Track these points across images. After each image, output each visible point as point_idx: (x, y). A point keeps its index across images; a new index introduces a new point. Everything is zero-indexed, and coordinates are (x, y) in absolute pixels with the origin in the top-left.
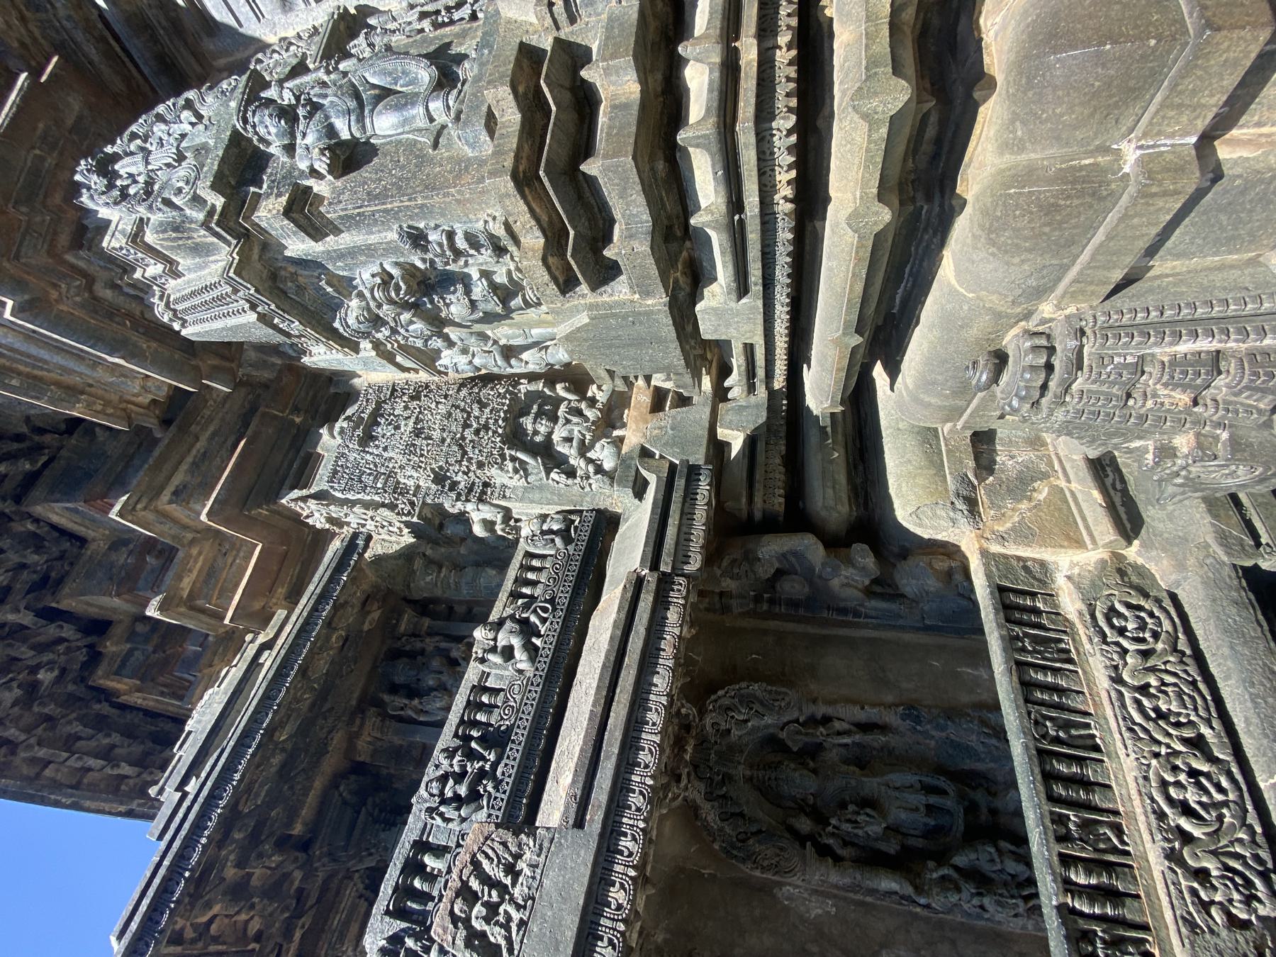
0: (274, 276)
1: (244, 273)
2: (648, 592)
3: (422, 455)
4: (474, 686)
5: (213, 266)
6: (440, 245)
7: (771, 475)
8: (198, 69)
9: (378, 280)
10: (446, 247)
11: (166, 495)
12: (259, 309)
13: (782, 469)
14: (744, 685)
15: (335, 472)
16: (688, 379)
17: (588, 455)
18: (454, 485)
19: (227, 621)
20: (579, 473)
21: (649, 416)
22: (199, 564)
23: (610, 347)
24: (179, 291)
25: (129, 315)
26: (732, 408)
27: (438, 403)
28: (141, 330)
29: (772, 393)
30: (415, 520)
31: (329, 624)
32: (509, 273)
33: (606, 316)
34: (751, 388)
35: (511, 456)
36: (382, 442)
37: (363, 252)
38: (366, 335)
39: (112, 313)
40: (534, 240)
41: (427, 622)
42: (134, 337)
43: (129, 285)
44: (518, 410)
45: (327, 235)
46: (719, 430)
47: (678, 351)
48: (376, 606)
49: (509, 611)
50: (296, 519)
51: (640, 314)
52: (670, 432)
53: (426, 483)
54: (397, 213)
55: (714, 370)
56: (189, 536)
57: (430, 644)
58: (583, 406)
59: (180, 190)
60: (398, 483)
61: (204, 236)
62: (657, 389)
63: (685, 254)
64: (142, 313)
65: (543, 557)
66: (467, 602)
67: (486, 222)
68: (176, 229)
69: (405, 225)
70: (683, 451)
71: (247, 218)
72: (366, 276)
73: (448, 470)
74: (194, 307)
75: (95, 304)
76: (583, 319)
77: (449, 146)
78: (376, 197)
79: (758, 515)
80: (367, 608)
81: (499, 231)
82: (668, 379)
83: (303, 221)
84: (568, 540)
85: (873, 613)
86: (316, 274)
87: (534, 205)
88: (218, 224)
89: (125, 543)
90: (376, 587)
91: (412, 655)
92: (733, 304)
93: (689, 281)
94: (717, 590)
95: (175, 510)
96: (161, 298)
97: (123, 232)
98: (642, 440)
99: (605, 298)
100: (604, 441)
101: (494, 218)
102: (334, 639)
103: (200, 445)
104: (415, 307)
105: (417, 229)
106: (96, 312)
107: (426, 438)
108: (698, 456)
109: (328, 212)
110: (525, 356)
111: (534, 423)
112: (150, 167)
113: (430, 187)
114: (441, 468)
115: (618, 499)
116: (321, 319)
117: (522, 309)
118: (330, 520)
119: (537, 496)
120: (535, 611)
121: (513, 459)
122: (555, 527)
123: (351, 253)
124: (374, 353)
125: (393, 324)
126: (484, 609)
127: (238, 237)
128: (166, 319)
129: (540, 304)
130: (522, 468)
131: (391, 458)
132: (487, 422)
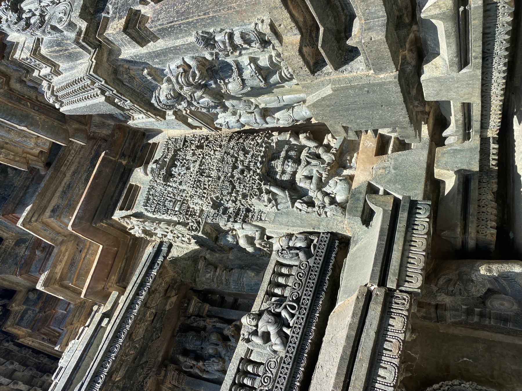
0: (115, 72)
1: (99, 71)
2: (376, 303)
3: (205, 188)
4: (242, 359)
5: (80, 67)
6: (224, 43)
7: (484, 210)
9: (181, 70)
10: (227, 45)
11: (48, 213)
12: (107, 94)
13: (494, 204)
14: (456, 382)
15: (148, 199)
16: (411, 131)
17: (324, 189)
18: (226, 209)
19: (82, 296)
20: (317, 203)
21: (375, 158)
22: (66, 257)
23: (347, 110)
24: (59, 84)
25: (29, 99)
26: (448, 152)
27: (215, 151)
28: (36, 108)
29: (484, 141)
30: (200, 234)
31: (145, 304)
32: (271, 57)
33: (347, 88)
34: (466, 136)
35: (266, 189)
36: (178, 179)
37: (172, 54)
38: (171, 107)
39: (20, 98)
40: (293, 38)
41: (207, 307)
42: (33, 113)
43: (30, 80)
44: (272, 155)
45: (149, 42)
46: (436, 170)
47: (404, 111)
48: (173, 293)
49: (265, 306)
50: (124, 231)
51: (374, 85)
52: (393, 171)
53: (207, 209)
54: (195, 24)
55: (431, 120)
56: (60, 239)
57: (209, 323)
58: (320, 151)
59: (61, 20)
60: (189, 207)
61: (75, 48)
62: (382, 136)
63: (412, 35)
64: (36, 97)
65: (290, 266)
66: (235, 294)
67: (256, 24)
68: (58, 45)
69: (200, 31)
70: (404, 188)
71: (101, 35)
72: (173, 67)
73: (222, 199)
74: (68, 94)
75: (11, 94)
76: (328, 91)
78: (182, 14)
79: (471, 243)
80: (168, 295)
81: (265, 29)
82: (394, 131)
83: (134, 34)
84: (308, 255)
86: (141, 68)
87: (294, 12)
88: (83, 41)
89: (24, 241)
90: (174, 280)
91: (198, 330)
92: (455, 74)
93: (415, 55)
94: (433, 303)
95: (53, 222)
96: (49, 89)
97: (28, 48)
98: (369, 179)
99: (346, 74)
100: (336, 179)
101: (263, 21)
102: (148, 315)
103: (67, 180)
104: (205, 87)
105: (208, 33)
106: (12, 99)
107: (207, 177)
108: (417, 193)
109: (151, 27)
110: (277, 115)
111: (283, 165)
112: (42, 4)
114: (217, 198)
115: (347, 225)
116: (144, 100)
117: (279, 83)
118: (145, 231)
119: (284, 219)
120: (285, 308)
121: (268, 192)
122: (299, 244)
123: (164, 54)
124: (174, 117)
125: (189, 99)
126: (246, 301)
127: (95, 48)
128: (51, 102)
129: (291, 79)
130: (274, 199)
131: (184, 190)
132: (249, 164)
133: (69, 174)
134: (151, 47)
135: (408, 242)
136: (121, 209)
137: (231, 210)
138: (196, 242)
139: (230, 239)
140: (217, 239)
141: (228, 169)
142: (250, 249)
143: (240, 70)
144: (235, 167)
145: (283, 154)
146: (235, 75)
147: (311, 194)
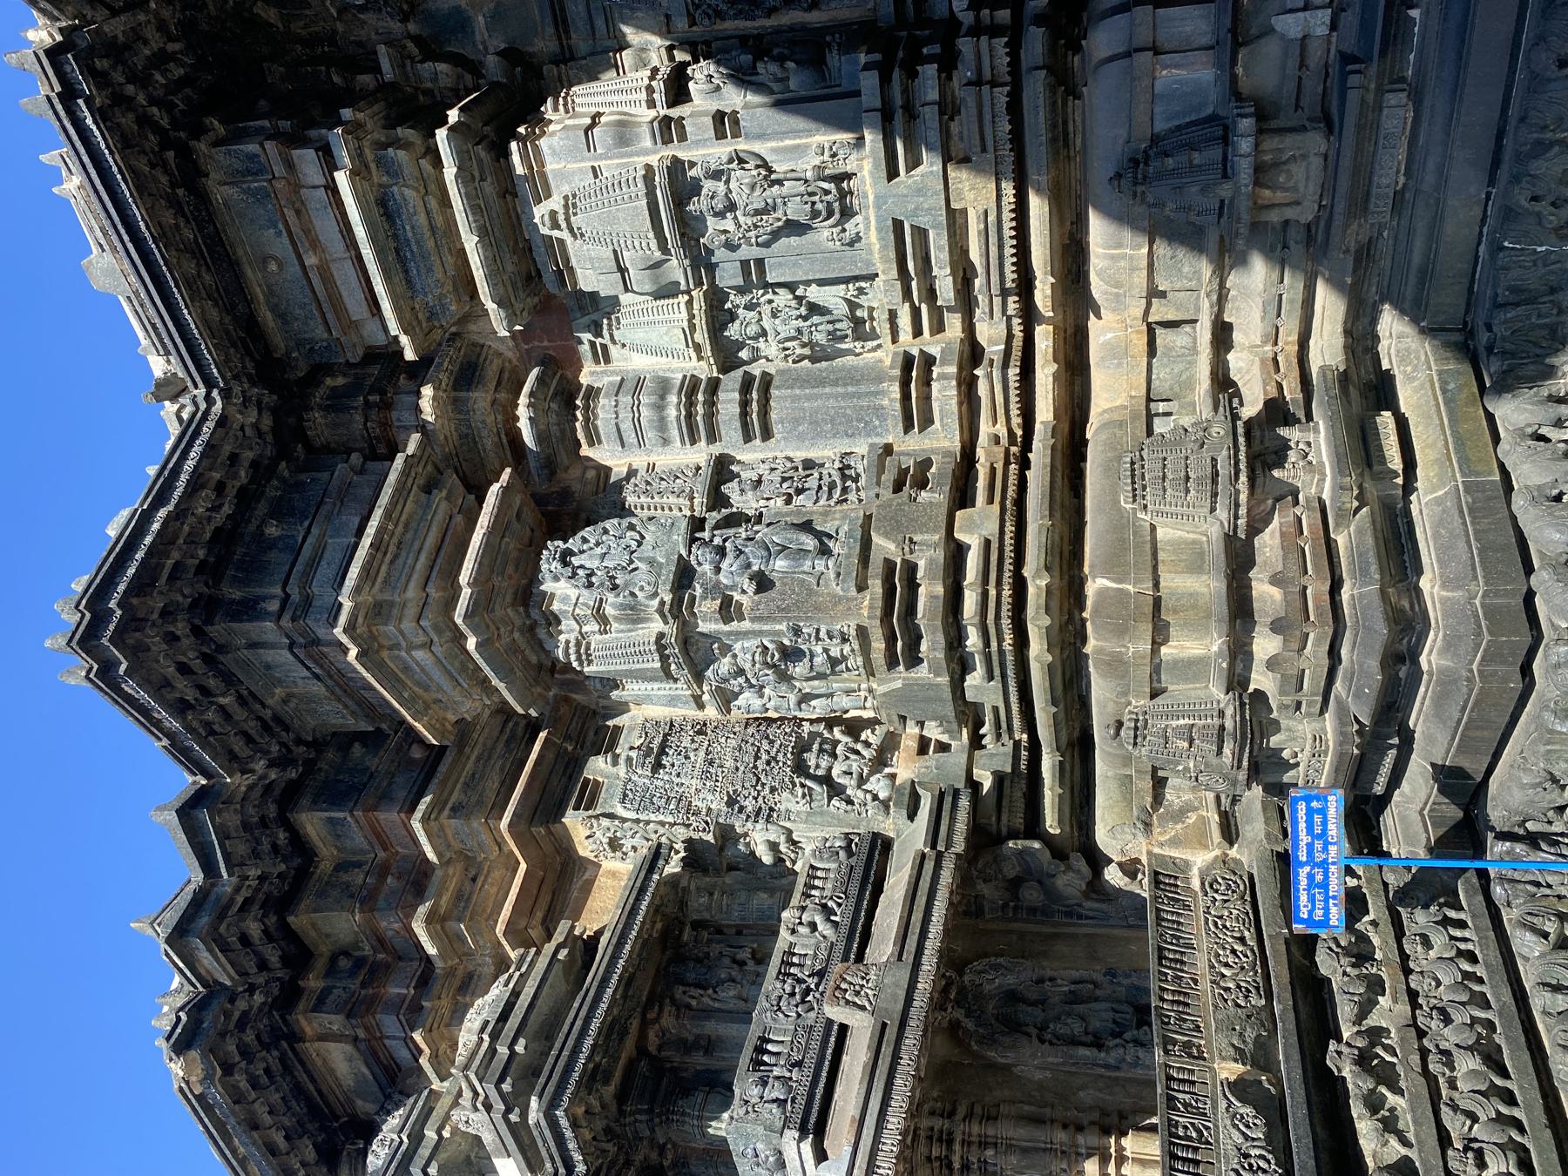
8: (566, 462)
11: (446, 812)
15: (625, 795)
44: (802, 747)
53: (718, 804)
56: (448, 855)
58: (859, 747)
76: (898, 684)
77: (827, 586)
79: (1004, 830)
84: (850, 854)
85: (1091, 914)
108: (961, 785)
110: (813, 703)
113: (817, 608)
115: (889, 825)
119: (819, 819)
121: (803, 786)
130: (809, 794)
133: (473, 758)
134: (735, 625)
135: (953, 819)
136: (576, 808)
137: (750, 808)
138: (683, 859)
139: (741, 847)
140: (722, 849)
141: (749, 759)
142: (767, 859)
143: (812, 656)
144: (757, 758)
145: (815, 747)
146: (806, 660)
147: (849, 792)
